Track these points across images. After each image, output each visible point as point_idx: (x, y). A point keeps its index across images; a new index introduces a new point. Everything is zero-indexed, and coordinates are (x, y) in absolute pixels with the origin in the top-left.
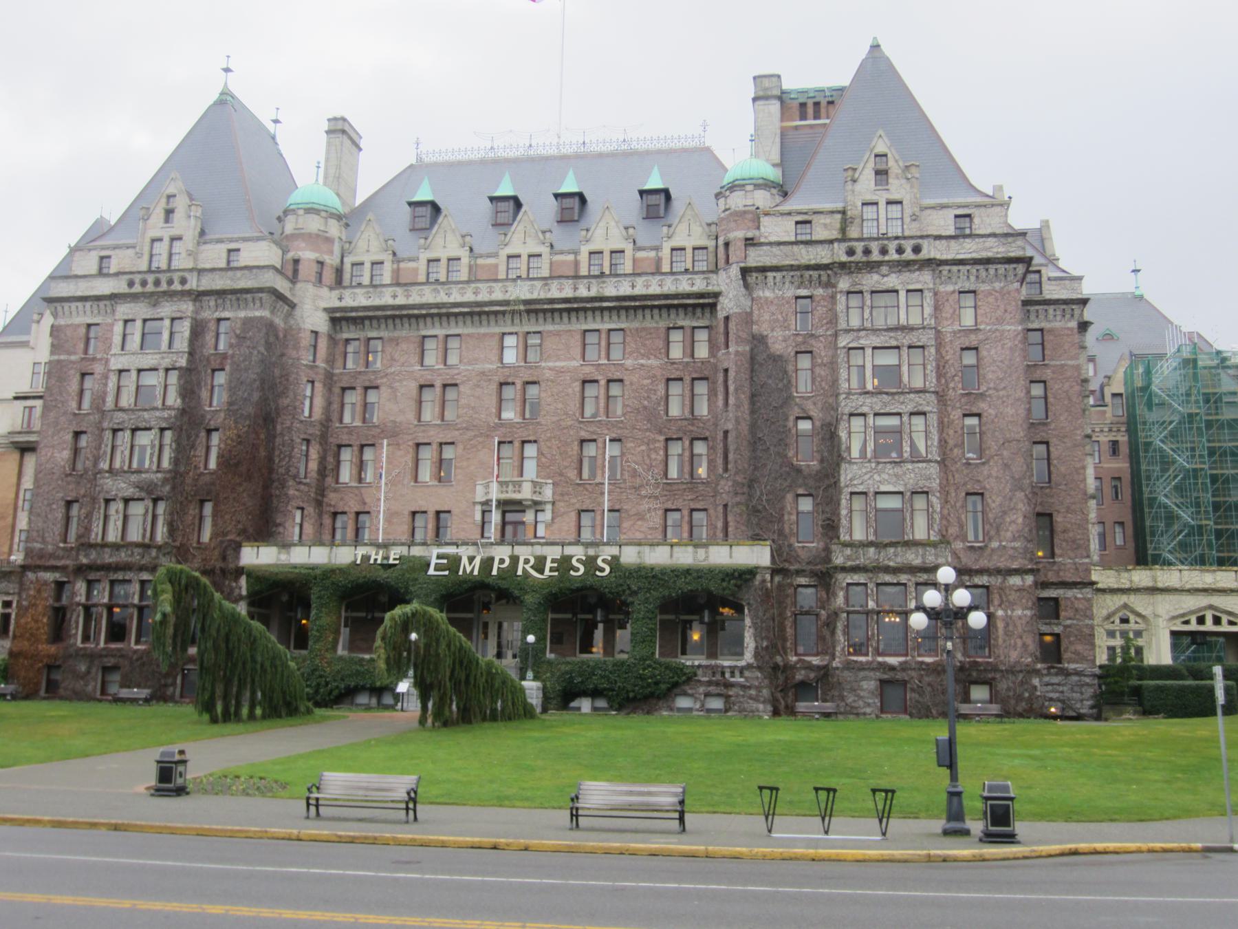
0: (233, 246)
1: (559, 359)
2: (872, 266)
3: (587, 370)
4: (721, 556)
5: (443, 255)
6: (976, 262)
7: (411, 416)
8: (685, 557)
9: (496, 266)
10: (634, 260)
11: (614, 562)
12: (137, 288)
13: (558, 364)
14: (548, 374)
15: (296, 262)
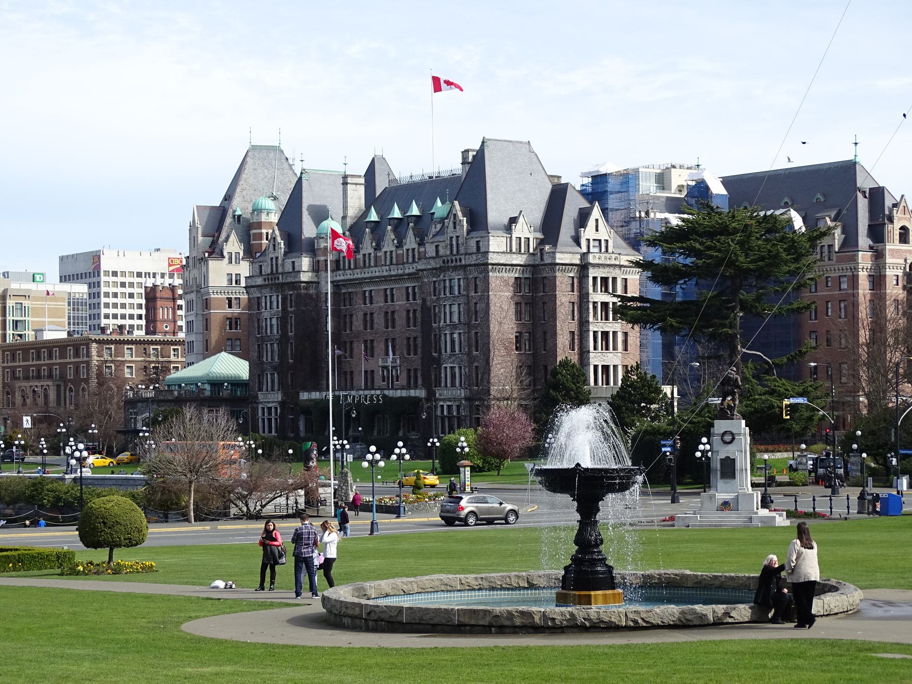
0: (293, 260)
1: (400, 301)
2: (448, 268)
3: (408, 305)
4: (413, 393)
5: (366, 252)
6: (475, 265)
7: (361, 328)
8: (404, 393)
9: (381, 256)
10: (419, 252)
11: (384, 396)
12: (267, 282)
13: (401, 303)
14: (397, 307)
15: (318, 261)
